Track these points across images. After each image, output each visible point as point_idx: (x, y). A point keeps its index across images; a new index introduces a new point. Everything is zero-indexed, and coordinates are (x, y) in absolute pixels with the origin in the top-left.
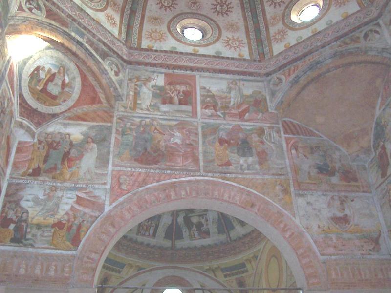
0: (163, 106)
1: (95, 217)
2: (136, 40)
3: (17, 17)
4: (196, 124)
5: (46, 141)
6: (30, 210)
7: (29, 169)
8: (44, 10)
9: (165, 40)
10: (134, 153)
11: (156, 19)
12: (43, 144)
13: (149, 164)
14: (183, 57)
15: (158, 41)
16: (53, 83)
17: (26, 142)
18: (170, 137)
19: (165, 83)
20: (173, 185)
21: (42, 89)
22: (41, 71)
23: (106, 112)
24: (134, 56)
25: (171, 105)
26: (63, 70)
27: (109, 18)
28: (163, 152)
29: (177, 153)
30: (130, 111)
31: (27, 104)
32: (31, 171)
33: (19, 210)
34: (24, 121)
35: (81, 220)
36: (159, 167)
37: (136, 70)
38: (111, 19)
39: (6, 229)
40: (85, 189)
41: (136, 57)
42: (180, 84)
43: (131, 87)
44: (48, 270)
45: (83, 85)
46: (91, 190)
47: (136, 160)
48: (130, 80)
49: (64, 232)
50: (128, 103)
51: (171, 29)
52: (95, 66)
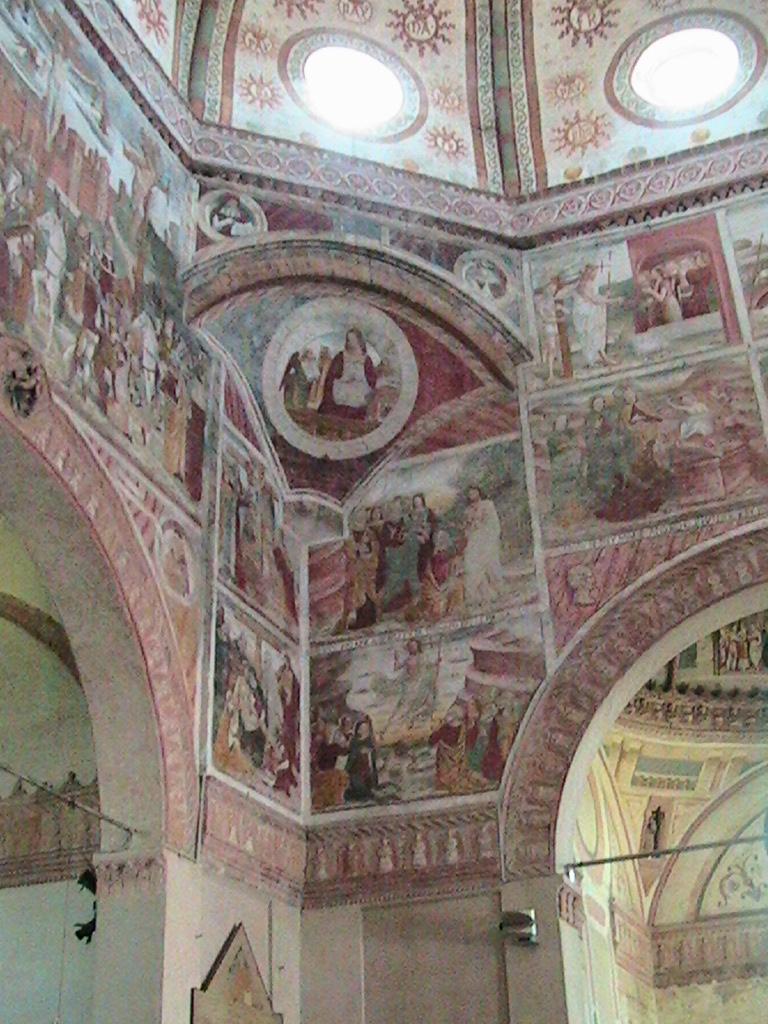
0: (639, 337)
1: (527, 693)
2: (531, 167)
3: (201, 268)
4: (741, 361)
5: (371, 528)
6: (372, 713)
7: (347, 613)
8: (260, 216)
9: (609, 138)
10: (590, 497)
11: (569, 81)
12: (365, 539)
13: (636, 516)
14: (668, 171)
15: (590, 145)
16: (345, 377)
17: (326, 547)
18: (677, 421)
19: (634, 263)
20: (710, 557)
21: (321, 407)
22: (304, 365)
23: (494, 404)
24: (536, 219)
25: (660, 328)
26: (357, 337)
27: (440, 141)
28: (667, 472)
29: (705, 463)
30: (558, 382)
31: (297, 452)
32: (353, 615)
33: (348, 719)
34: (305, 498)
35: (495, 710)
36: (665, 517)
37: (547, 258)
38: (445, 140)
39: (331, 772)
40: (490, 626)
41: (540, 220)
42: (678, 253)
43: (545, 310)
44: (443, 850)
45: (419, 355)
46: (504, 625)
47: (600, 515)
48: (538, 292)
49: (460, 751)
50: (547, 361)
51: (618, 94)
52: (436, 294)
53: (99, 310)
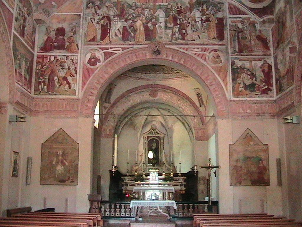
34: (265, 18)
53: (178, 19)
